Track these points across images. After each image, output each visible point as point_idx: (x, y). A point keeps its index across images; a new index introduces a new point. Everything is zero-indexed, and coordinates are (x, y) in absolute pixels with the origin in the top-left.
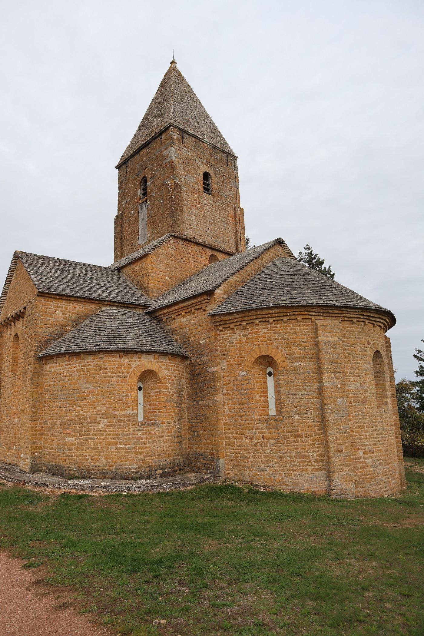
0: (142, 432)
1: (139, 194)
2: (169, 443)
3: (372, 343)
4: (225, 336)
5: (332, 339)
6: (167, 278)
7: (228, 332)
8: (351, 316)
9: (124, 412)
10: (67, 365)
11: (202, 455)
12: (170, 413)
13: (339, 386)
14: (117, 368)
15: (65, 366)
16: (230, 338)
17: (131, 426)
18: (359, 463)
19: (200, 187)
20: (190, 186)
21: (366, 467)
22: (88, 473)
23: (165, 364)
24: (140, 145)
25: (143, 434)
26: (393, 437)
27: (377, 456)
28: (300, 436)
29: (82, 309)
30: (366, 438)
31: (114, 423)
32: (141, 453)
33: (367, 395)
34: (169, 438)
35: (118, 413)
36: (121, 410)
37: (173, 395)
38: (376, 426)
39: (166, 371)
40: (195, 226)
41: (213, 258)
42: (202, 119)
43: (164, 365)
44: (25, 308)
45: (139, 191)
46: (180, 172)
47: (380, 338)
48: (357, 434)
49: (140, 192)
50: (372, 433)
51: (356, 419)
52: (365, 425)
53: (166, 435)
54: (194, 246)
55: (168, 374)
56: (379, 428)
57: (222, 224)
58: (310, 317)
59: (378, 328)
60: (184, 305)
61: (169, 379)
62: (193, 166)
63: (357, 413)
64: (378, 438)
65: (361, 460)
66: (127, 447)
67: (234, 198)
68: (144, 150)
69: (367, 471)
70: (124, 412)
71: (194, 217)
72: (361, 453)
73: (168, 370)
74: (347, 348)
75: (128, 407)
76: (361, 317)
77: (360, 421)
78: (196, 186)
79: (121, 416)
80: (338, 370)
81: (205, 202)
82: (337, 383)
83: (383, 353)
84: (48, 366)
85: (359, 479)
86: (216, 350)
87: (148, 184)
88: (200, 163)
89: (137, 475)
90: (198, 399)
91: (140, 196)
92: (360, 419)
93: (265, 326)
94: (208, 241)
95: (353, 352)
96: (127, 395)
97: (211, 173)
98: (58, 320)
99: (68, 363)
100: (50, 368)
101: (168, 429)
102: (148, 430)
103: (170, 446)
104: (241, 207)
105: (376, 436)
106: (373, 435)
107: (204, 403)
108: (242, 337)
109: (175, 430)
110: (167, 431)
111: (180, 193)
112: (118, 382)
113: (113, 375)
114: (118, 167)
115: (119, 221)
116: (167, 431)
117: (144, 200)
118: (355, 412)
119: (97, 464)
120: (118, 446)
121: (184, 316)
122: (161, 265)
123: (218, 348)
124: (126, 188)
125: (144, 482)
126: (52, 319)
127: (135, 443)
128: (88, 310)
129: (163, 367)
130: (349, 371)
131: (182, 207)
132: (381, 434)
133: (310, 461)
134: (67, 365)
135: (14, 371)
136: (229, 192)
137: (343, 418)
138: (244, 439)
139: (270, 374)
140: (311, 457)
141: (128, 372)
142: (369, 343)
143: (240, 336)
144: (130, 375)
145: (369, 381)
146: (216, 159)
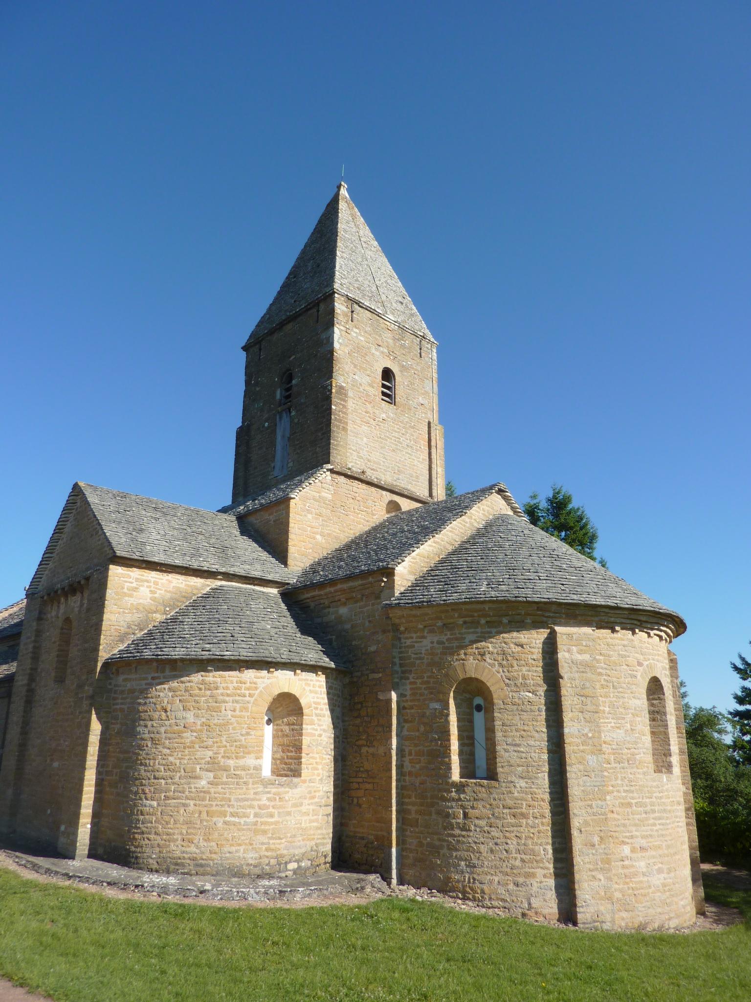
0: (269, 795)
1: (278, 396)
2: (311, 817)
3: (645, 663)
4: (408, 642)
5: (580, 657)
6: (318, 537)
7: (414, 635)
8: (612, 619)
9: (241, 762)
10: (153, 678)
11: (363, 838)
12: (315, 765)
13: (590, 735)
14: (235, 688)
15: (150, 681)
16: (416, 645)
17: (250, 786)
18: (623, 867)
21: (635, 874)
22: (176, 864)
23: (312, 683)
24: (284, 317)
25: (269, 799)
26: (680, 824)
27: (654, 857)
28: (524, 816)
29: (181, 586)
30: (636, 825)
31: (225, 779)
32: (265, 832)
33: (636, 751)
34: (311, 807)
35: (231, 763)
36: (237, 758)
37: (320, 735)
38: (652, 804)
39: (313, 695)
40: (366, 453)
41: (393, 506)
42: (383, 280)
43: (309, 685)
44: (87, 579)
45: (278, 392)
47: (659, 655)
48: (619, 817)
49: (281, 394)
50: (644, 815)
51: (618, 791)
52: (633, 801)
53: (307, 802)
54: (364, 486)
55: (315, 700)
56: (656, 808)
58: (545, 619)
59: (657, 638)
60: (345, 586)
61: (316, 709)
62: (367, 358)
63: (619, 782)
64: (655, 825)
65: (626, 863)
66: (242, 821)
67: (429, 409)
68: (289, 326)
69: (636, 883)
70: (241, 762)
71: (365, 439)
72: (626, 850)
73: (316, 693)
74: (604, 671)
75: (249, 753)
76: (628, 621)
77: (624, 794)
78: (368, 388)
79: (236, 768)
80: (590, 707)
81: (384, 416)
82: (586, 731)
83: (666, 682)
84: (121, 678)
85: (623, 895)
86: (394, 664)
87: (294, 382)
88: (378, 353)
89: (257, 871)
90: (360, 742)
91: (280, 400)
92: (625, 791)
93: (472, 630)
94: (386, 478)
95: (615, 679)
96: (248, 734)
97: (395, 369)
98: (141, 601)
99: (156, 675)
100: (125, 680)
101: (310, 792)
102: (278, 794)
103: (311, 821)
105: (651, 821)
106: (647, 819)
107: (371, 750)
108: (435, 644)
109: (321, 793)
110: (308, 796)
112: (234, 711)
113: (227, 699)
114: (245, 348)
115: (243, 436)
116: (308, 796)
117: (286, 406)
118: (616, 779)
119: (193, 849)
120: (228, 819)
121: (345, 604)
122: (310, 516)
123: (397, 660)
124: (257, 384)
125: (267, 883)
126: (131, 600)
127: (256, 815)
128: (191, 586)
129: (307, 688)
130: (607, 709)
131: (346, 423)
132: (660, 819)
133: (541, 861)
134: (153, 678)
135: (60, 680)
136: (421, 400)
137: (596, 789)
138: (434, 816)
139: (479, 708)
140: (542, 852)
141: (250, 695)
142: (640, 664)
143: (432, 643)
144: (256, 700)
145: (639, 727)
146: (403, 346)
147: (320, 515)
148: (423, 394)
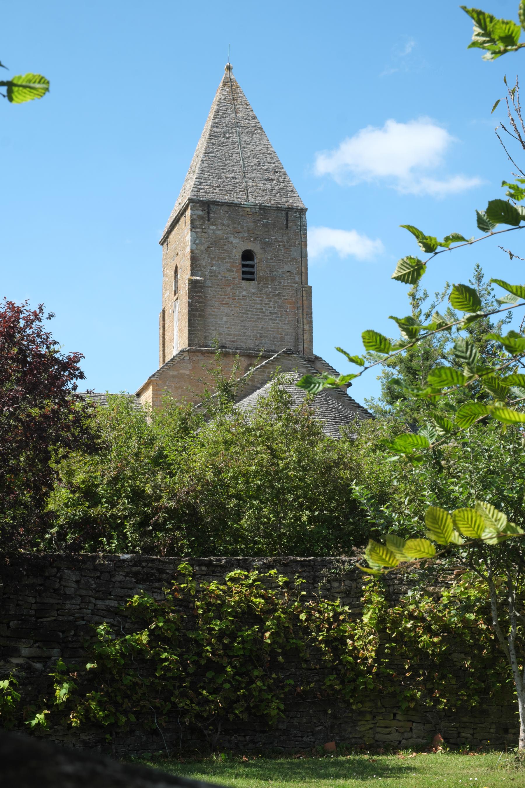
19: (237, 275)
20: (220, 276)
46: (204, 263)
57: (273, 316)
67: (297, 274)
71: (225, 319)
81: (244, 293)
88: (237, 240)
104: (309, 284)
111: (201, 292)
136: (287, 268)
147: (179, 388)
148: (290, 261)
